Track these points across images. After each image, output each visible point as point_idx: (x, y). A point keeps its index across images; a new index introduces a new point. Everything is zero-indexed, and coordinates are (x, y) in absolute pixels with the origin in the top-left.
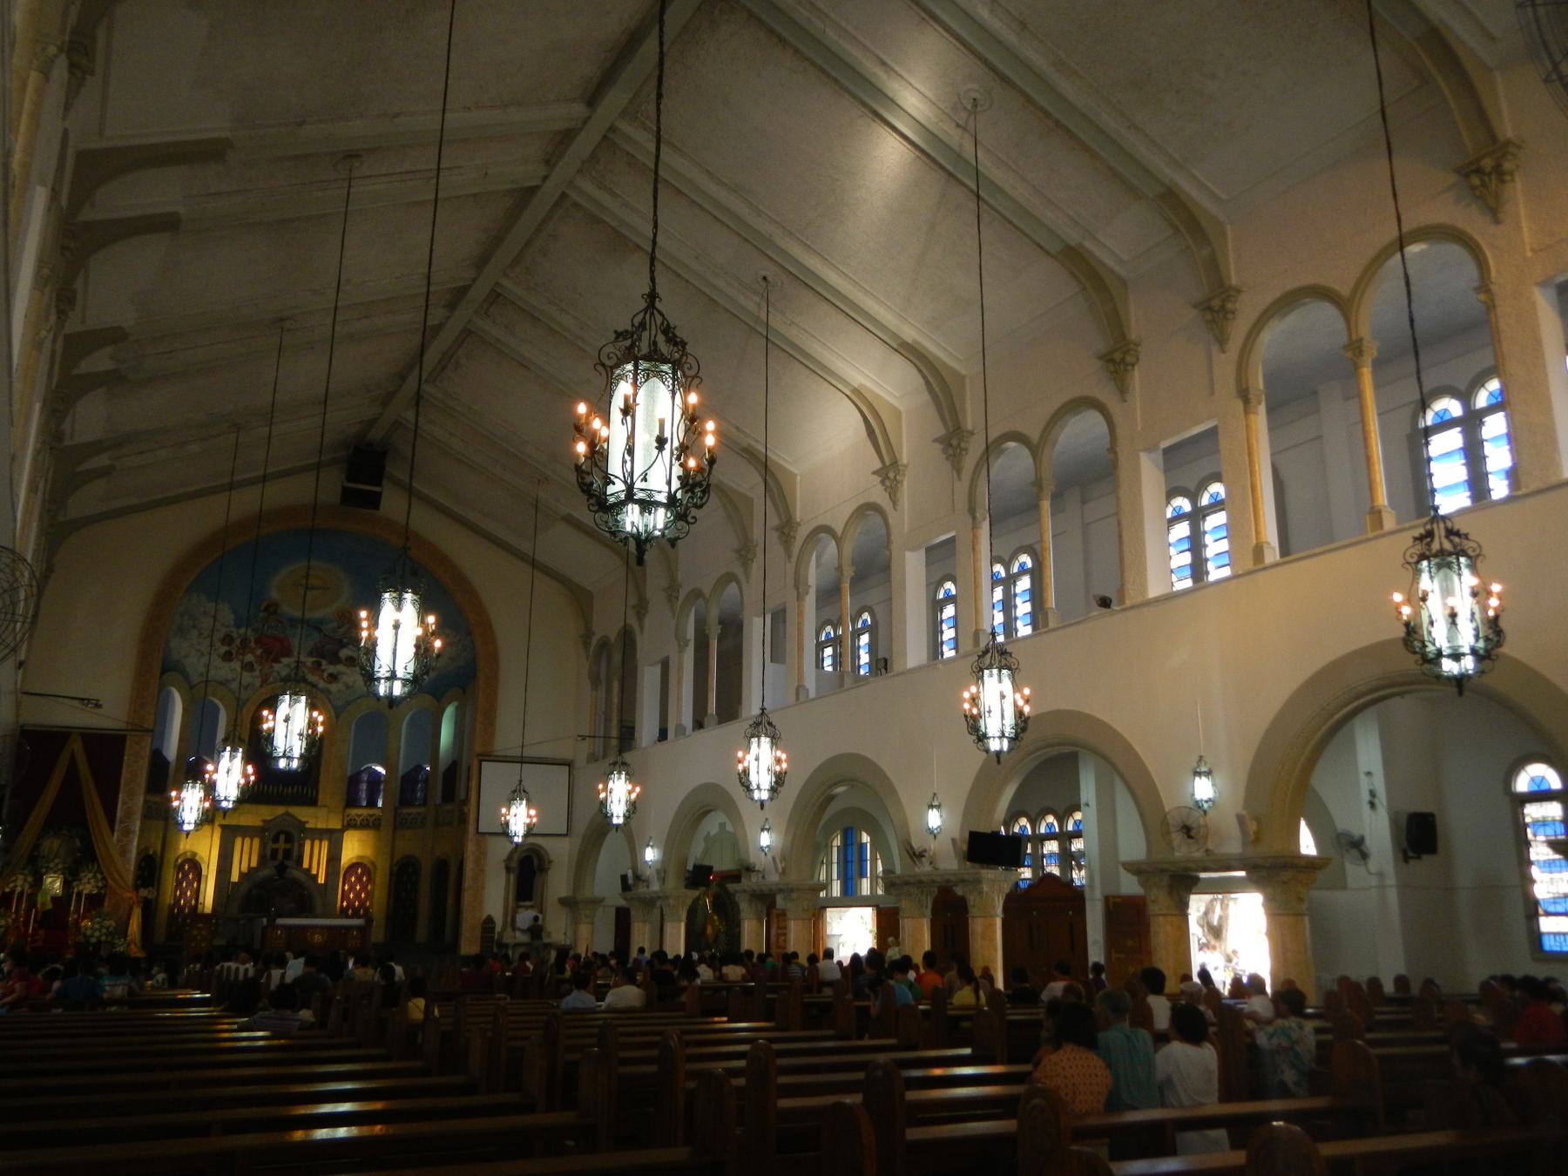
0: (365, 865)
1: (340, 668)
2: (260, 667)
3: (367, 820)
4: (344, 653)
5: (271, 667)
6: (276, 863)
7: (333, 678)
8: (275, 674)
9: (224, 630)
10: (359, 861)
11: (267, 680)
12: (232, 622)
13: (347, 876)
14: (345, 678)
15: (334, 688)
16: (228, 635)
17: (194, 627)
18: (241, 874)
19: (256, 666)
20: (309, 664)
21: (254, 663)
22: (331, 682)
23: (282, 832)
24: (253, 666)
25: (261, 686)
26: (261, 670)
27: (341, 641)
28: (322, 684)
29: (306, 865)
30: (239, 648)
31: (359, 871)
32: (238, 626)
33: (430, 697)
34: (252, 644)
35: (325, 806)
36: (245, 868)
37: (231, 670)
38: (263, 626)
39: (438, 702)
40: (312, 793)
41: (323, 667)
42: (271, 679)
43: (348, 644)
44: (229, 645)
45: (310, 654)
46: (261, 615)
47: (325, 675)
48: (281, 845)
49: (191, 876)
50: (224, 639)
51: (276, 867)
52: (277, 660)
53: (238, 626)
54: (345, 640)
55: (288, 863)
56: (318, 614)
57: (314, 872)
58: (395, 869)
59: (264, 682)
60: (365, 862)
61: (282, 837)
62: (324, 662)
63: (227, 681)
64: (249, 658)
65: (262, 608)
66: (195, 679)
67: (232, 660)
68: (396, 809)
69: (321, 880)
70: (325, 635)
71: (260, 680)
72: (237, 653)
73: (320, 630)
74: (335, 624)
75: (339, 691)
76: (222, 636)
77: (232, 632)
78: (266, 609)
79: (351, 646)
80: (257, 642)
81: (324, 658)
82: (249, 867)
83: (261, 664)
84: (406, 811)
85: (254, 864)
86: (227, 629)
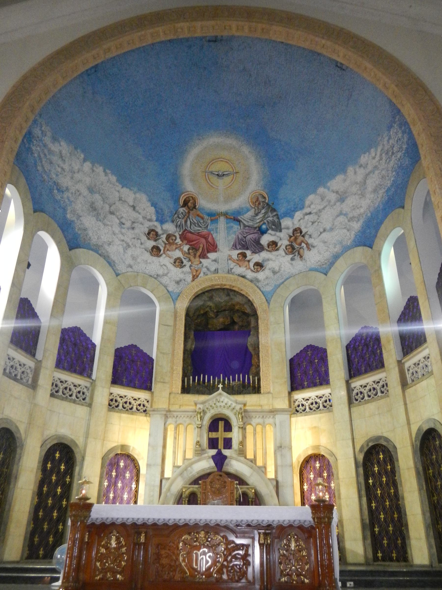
0: (324, 456)
1: (264, 255)
2: (190, 263)
3: (316, 403)
4: (265, 240)
5: (201, 263)
6: (213, 452)
7: (259, 266)
8: (204, 270)
9: (148, 224)
10: (316, 452)
11: (198, 276)
12: (154, 218)
13: (305, 472)
14: (270, 265)
15: (261, 275)
16: (153, 230)
17: (112, 213)
18: (175, 467)
19: (185, 262)
20: (235, 257)
21: (183, 260)
22: (258, 271)
23: (221, 419)
24: (182, 263)
25: (193, 280)
26: (191, 266)
27: (260, 228)
28: (250, 275)
29: (250, 455)
30: (165, 244)
31: (318, 465)
32: (162, 221)
33: (360, 249)
34: (178, 241)
35: (269, 393)
36: (180, 462)
37: (161, 266)
38: (186, 222)
39: (371, 248)
40: (254, 381)
41: (248, 258)
42: (202, 274)
43: (267, 230)
44: (155, 240)
45: (235, 247)
46: (181, 210)
47: (251, 264)
48: (221, 434)
49: (128, 475)
50: (149, 233)
51: (213, 457)
52: (203, 256)
53: (162, 221)
54: (264, 227)
55: (226, 452)
56: (234, 205)
57: (260, 463)
58: (361, 457)
59: (195, 277)
60: (322, 453)
61: (221, 425)
62: (248, 253)
63: (157, 275)
64: (178, 254)
65: (181, 202)
66: (122, 268)
67: (161, 256)
68: (348, 384)
69: (271, 475)
70: (245, 226)
71: (191, 277)
72: (165, 248)
73: (239, 221)
74: (251, 213)
75: (267, 278)
76: (147, 231)
77: (156, 227)
78: (185, 204)
79: (270, 231)
80: (183, 237)
81: (247, 249)
82: (185, 459)
83: (190, 260)
84: (357, 383)
85: (190, 455)
86: (151, 224)
